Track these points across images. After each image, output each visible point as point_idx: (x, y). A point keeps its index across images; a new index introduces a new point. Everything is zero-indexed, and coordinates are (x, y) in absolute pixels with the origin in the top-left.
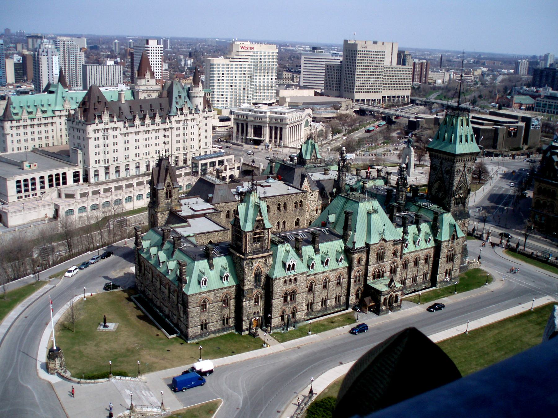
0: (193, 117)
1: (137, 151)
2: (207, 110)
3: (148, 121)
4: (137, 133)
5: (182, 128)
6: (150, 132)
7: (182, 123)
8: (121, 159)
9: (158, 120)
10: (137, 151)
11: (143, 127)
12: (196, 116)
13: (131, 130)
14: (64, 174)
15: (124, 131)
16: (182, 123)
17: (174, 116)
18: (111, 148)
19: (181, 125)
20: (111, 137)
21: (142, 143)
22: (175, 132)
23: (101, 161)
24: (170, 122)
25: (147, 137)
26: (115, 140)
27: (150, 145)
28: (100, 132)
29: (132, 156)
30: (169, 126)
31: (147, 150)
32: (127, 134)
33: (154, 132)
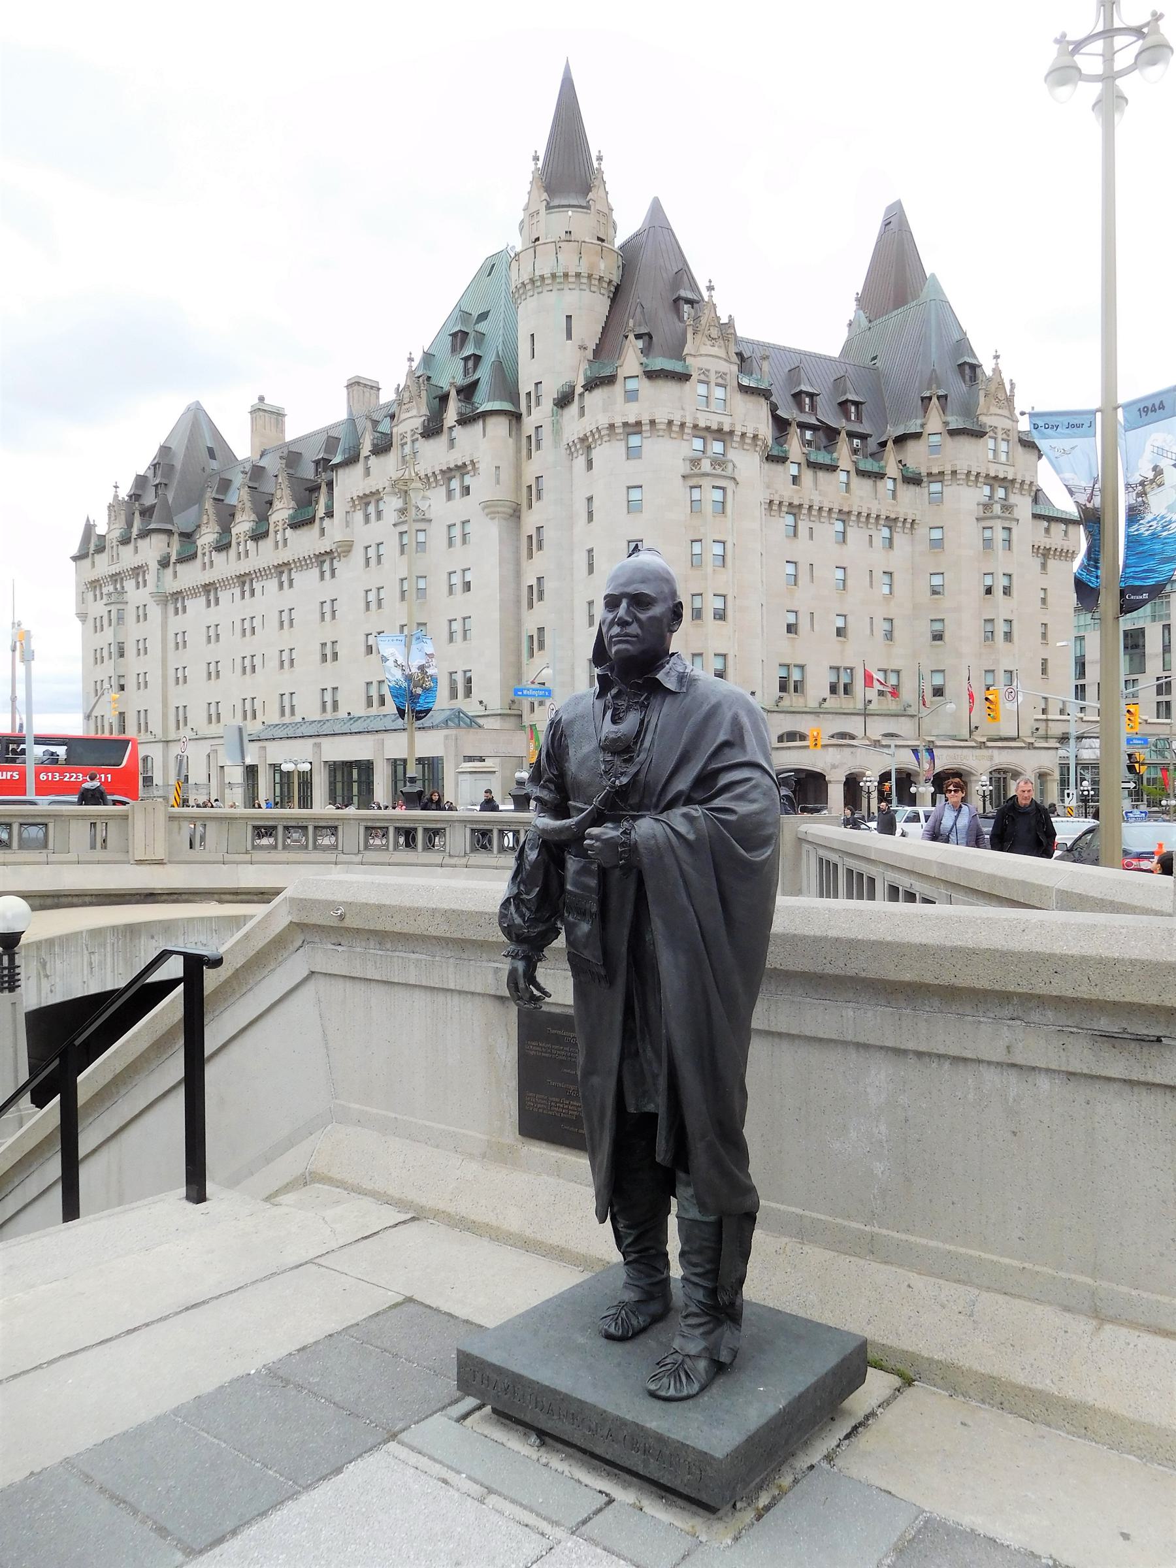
3: (243, 525)
5: (390, 549)
9: (281, 512)
13: (190, 575)
19: (383, 530)
24: (330, 514)
27: (258, 661)
33: (272, 584)
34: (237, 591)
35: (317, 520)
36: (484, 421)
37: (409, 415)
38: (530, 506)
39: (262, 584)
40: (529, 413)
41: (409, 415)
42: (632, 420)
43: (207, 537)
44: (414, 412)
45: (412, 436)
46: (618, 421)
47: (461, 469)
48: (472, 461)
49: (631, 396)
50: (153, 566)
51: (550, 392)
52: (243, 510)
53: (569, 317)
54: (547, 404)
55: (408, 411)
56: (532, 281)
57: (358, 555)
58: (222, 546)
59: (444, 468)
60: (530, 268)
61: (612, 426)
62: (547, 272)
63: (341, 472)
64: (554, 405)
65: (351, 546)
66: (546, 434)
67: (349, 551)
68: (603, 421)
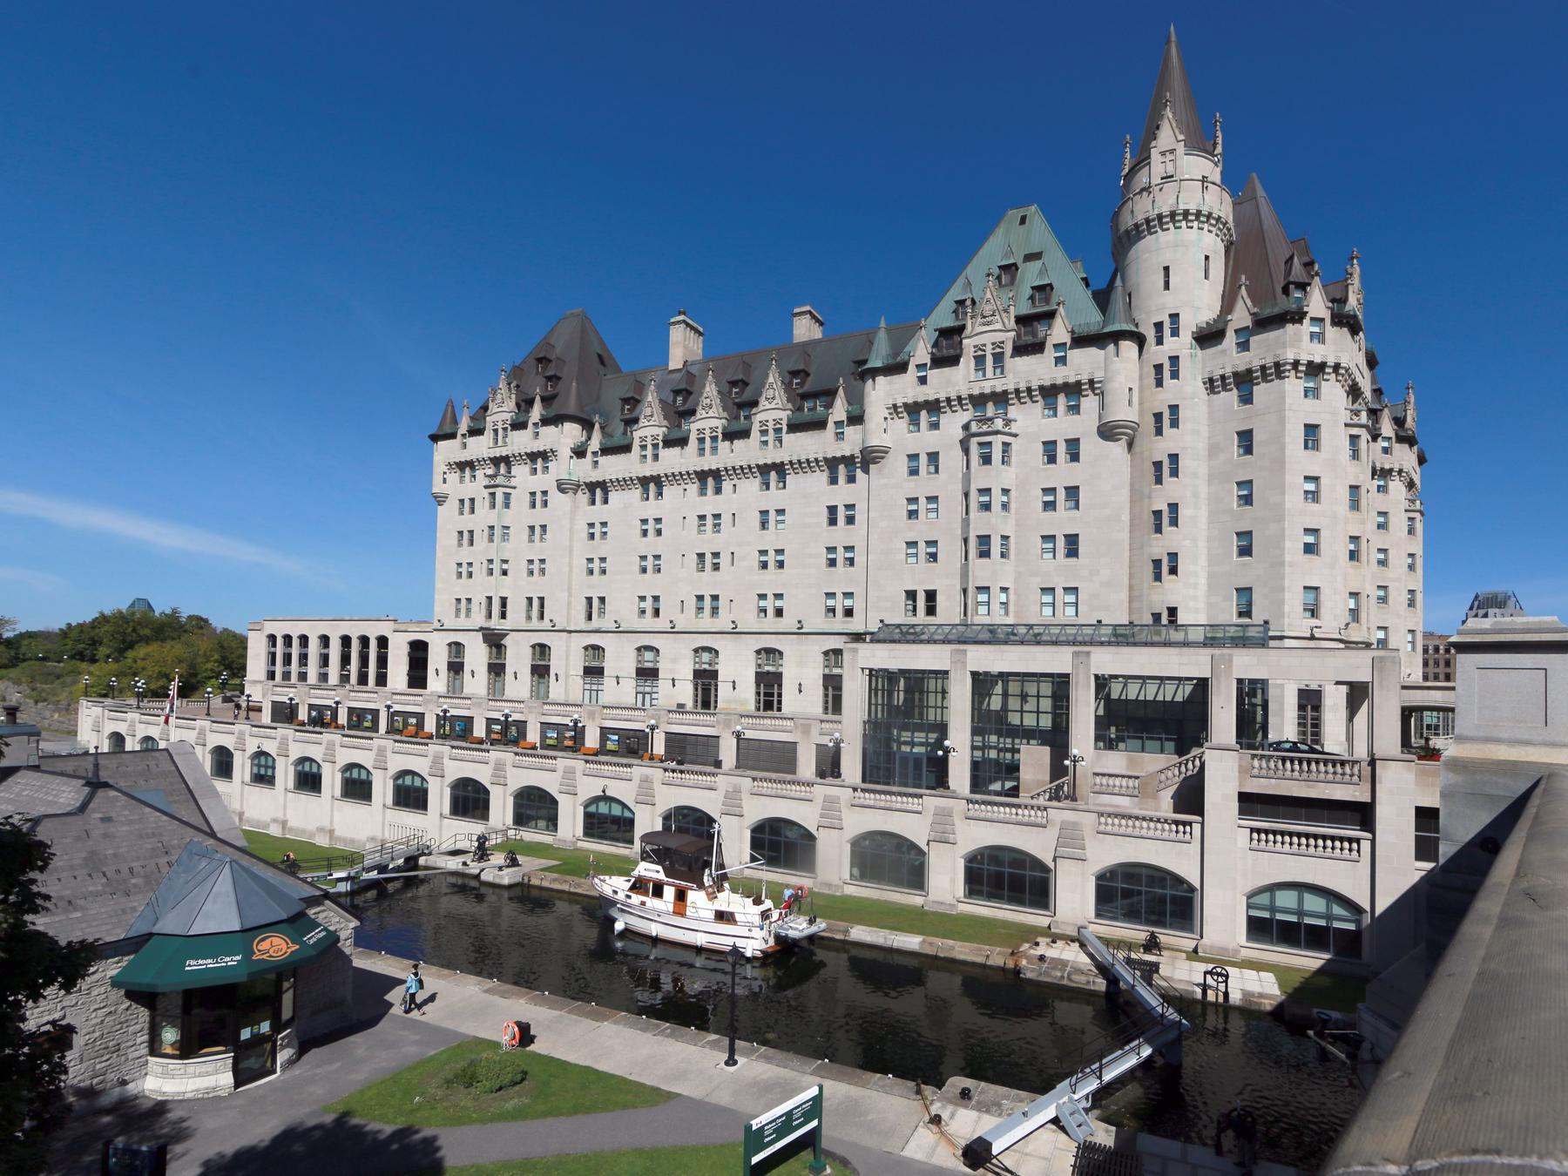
0: (1062, 375)
1: (651, 585)
2: (1241, 316)
4: (652, 484)
5: (952, 460)
6: (727, 486)
7: (953, 423)
8: (565, 609)
9: (773, 408)
10: (651, 585)
11: (676, 451)
12: (1084, 363)
14: (383, 642)
15: (583, 470)
16: (953, 423)
17: (874, 373)
18: (518, 549)
20: (520, 499)
21: (682, 539)
22: (889, 482)
23: (474, 607)
24: (856, 419)
25: (708, 511)
26: (538, 516)
27: (724, 561)
28: (479, 474)
29: (623, 609)
30: (853, 440)
31: (708, 583)
32: (598, 489)
33: (752, 485)
34: (693, 488)
35: (830, 425)
36: (1116, 345)
37: (987, 328)
38: (1159, 432)
39: (733, 482)
40: (1160, 341)
41: (987, 328)
42: (1318, 360)
43: (651, 427)
44: (999, 326)
45: (993, 349)
46: (1304, 358)
47: (1074, 390)
48: (1091, 382)
49: (1319, 337)
50: (565, 452)
51: (1189, 325)
52: (711, 407)
53: (1207, 258)
54: (1186, 336)
55: (988, 324)
56: (1173, 215)
57: (896, 465)
58: (676, 441)
59: (1047, 383)
60: (1172, 201)
61: (1296, 364)
62: (1193, 208)
63: (880, 380)
64: (1194, 338)
65: (887, 452)
66: (1184, 365)
67: (883, 458)
68: (1290, 356)
